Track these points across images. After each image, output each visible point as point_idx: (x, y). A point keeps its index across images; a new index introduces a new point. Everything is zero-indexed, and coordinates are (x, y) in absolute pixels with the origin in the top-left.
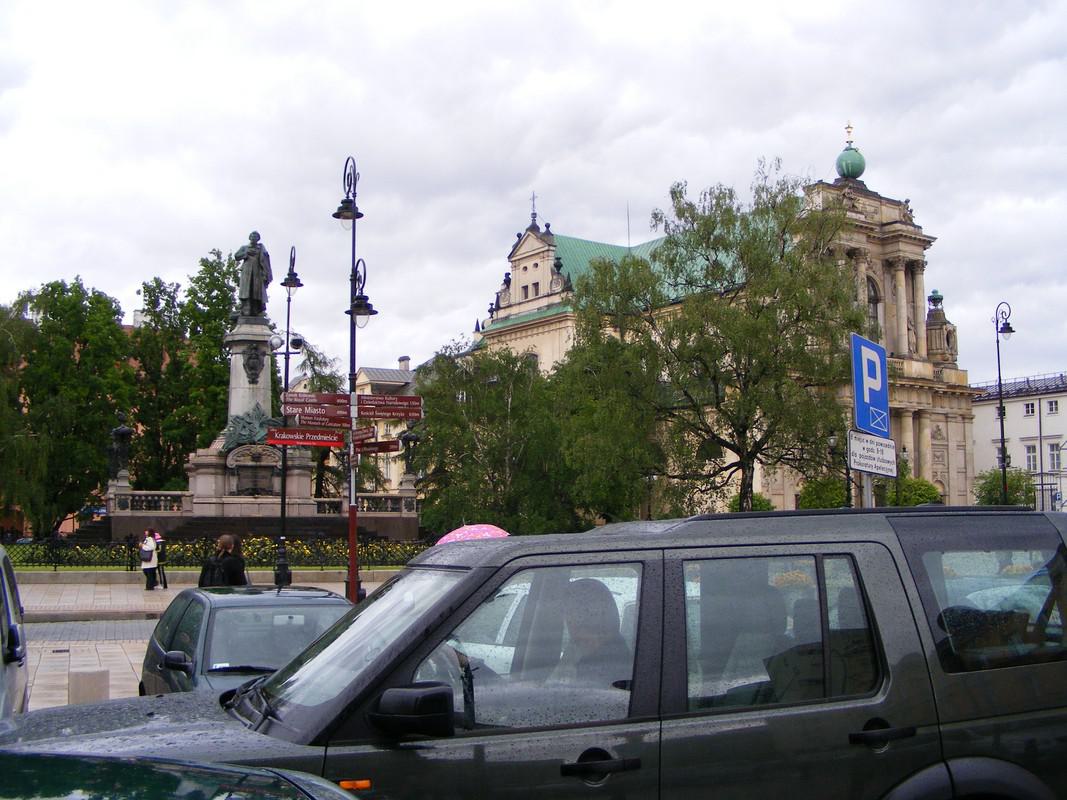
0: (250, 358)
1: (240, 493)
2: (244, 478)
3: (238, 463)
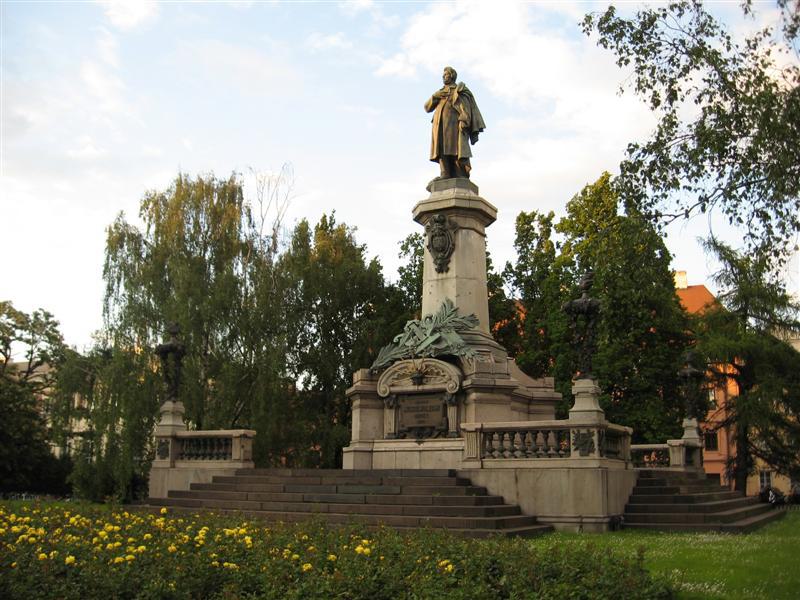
0: (432, 237)
1: (400, 435)
2: (409, 410)
3: (392, 389)
